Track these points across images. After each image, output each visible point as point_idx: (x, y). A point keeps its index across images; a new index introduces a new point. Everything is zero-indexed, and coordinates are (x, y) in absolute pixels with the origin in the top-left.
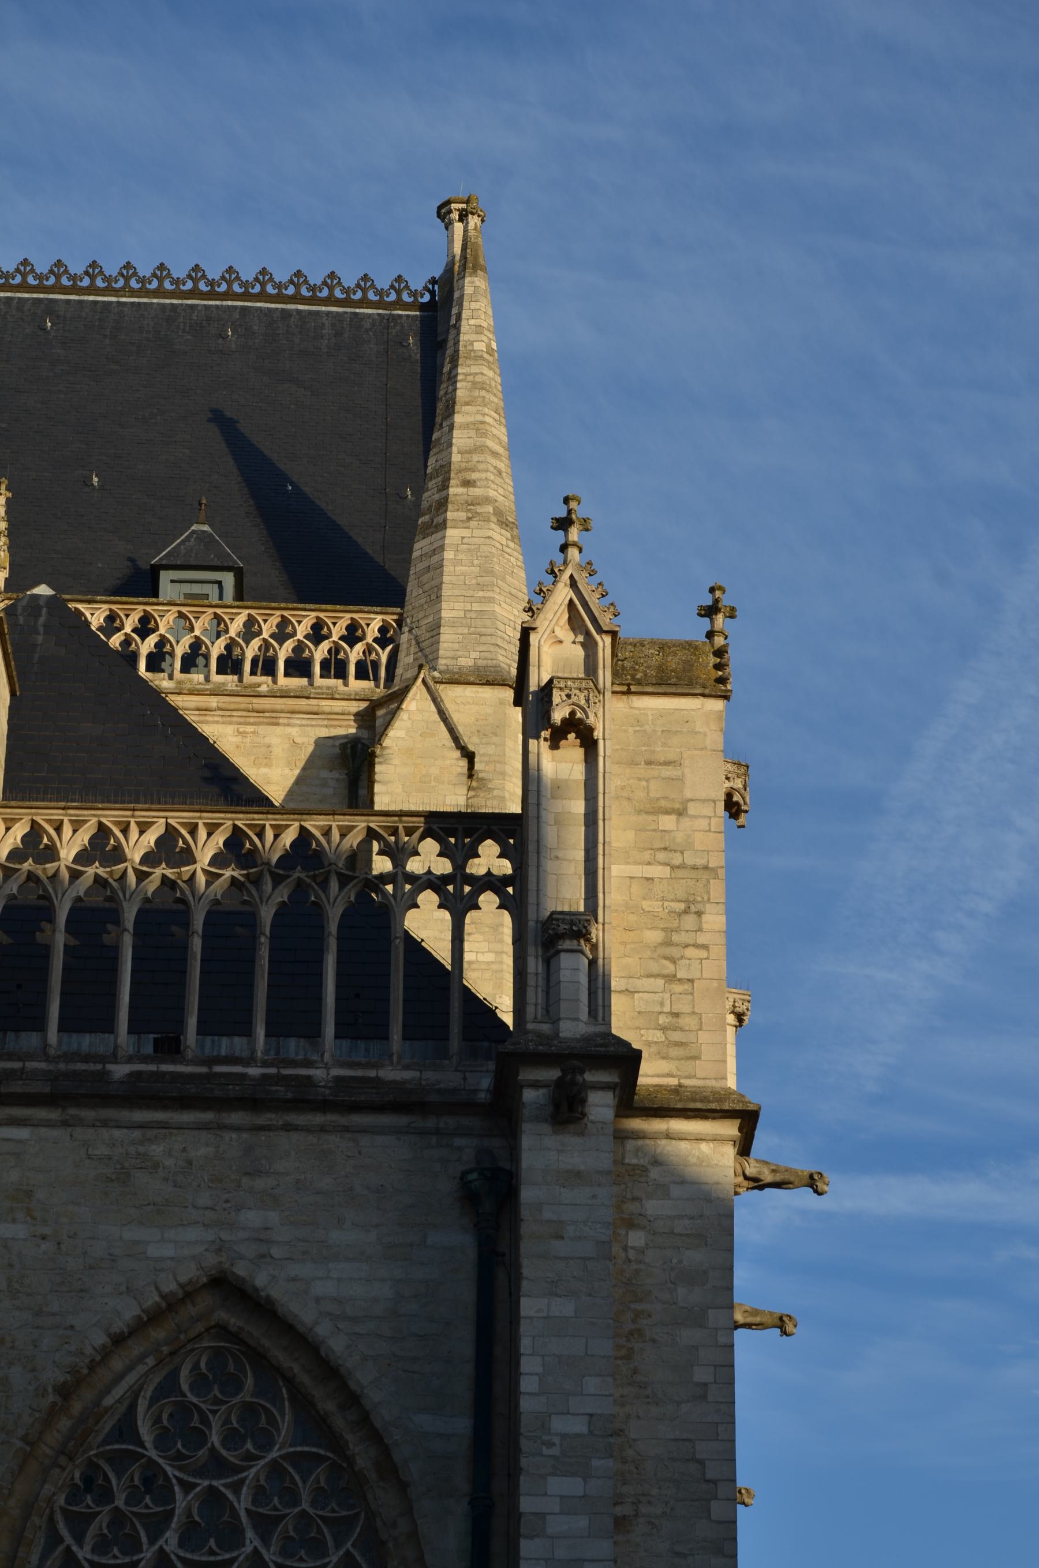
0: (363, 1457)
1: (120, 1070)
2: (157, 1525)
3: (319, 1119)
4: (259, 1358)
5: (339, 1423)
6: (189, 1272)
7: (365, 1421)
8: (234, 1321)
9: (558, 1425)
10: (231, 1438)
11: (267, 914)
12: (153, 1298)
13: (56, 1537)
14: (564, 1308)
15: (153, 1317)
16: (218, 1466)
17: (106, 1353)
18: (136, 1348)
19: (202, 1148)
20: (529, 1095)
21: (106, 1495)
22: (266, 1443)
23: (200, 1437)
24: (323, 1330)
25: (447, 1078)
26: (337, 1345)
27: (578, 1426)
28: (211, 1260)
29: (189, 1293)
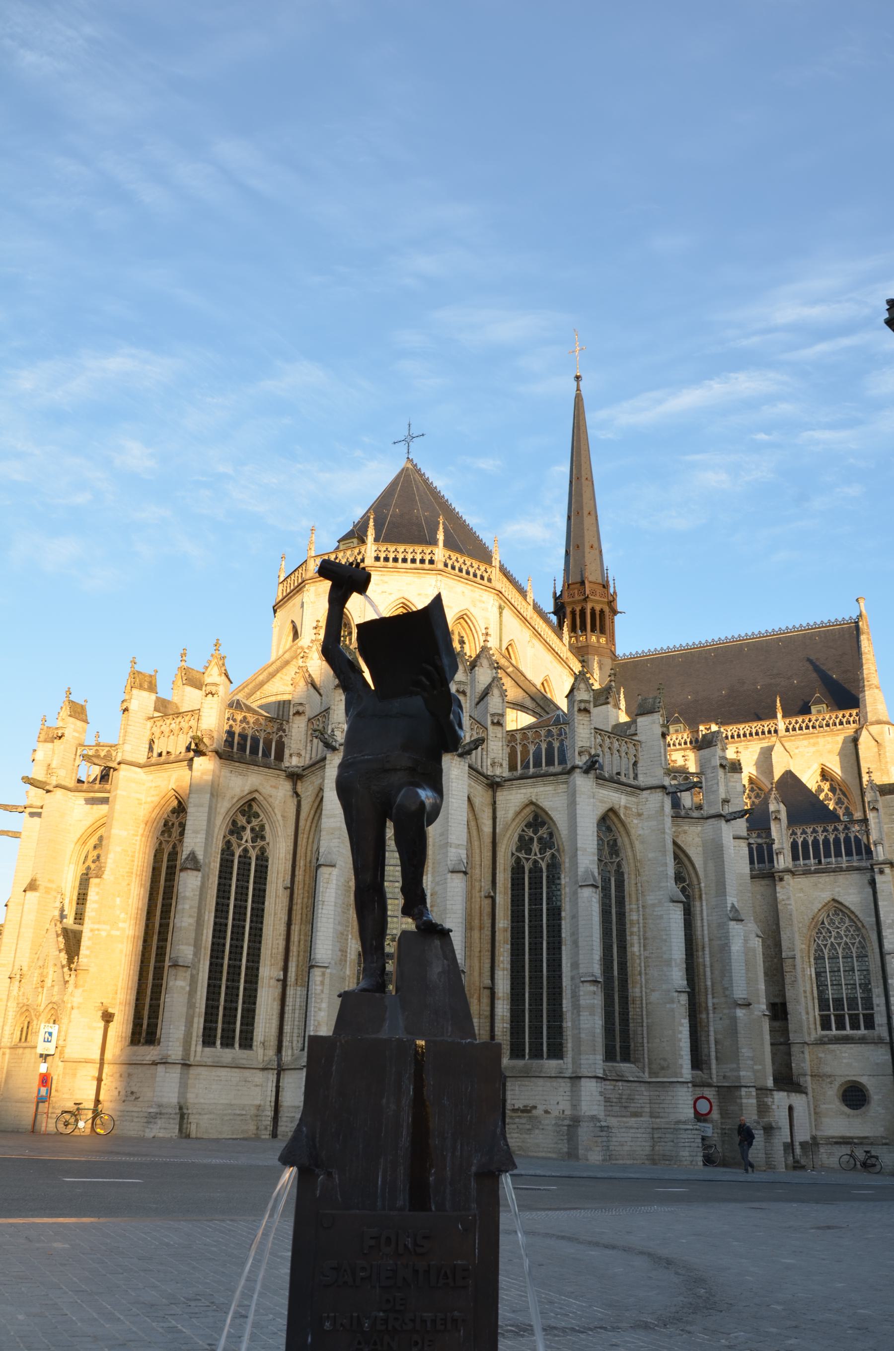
0: (860, 925)
1: (813, 868)
2: (830, 937)
3: (844, 873)
4: (841, 910)
5: (855, 920)
6: (829, 899)
7: (859, 919)
8: (837, 905)
9: (887, 921)
10: (839, 923)
11: (831, 840)
12: (824, 904)
13: (815, 941)
14: (885, 903)
15: (824, 906)
16: (838, 928)
17: (818, 912)
18: (822, 911)
19: (827, 879)
20: (875, 870)
21: (821, 933)
22: (845, 924)
23: (834, 923)
24: (850, 906)
25: (864, 864)
26: (853, 908)
27: (890, 921)
28: (832, 897)
29: (829, 902)
